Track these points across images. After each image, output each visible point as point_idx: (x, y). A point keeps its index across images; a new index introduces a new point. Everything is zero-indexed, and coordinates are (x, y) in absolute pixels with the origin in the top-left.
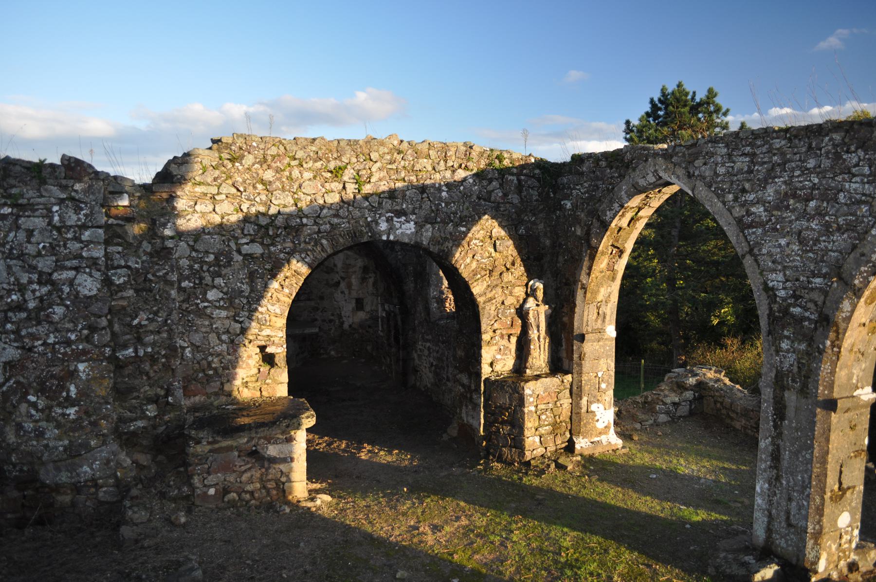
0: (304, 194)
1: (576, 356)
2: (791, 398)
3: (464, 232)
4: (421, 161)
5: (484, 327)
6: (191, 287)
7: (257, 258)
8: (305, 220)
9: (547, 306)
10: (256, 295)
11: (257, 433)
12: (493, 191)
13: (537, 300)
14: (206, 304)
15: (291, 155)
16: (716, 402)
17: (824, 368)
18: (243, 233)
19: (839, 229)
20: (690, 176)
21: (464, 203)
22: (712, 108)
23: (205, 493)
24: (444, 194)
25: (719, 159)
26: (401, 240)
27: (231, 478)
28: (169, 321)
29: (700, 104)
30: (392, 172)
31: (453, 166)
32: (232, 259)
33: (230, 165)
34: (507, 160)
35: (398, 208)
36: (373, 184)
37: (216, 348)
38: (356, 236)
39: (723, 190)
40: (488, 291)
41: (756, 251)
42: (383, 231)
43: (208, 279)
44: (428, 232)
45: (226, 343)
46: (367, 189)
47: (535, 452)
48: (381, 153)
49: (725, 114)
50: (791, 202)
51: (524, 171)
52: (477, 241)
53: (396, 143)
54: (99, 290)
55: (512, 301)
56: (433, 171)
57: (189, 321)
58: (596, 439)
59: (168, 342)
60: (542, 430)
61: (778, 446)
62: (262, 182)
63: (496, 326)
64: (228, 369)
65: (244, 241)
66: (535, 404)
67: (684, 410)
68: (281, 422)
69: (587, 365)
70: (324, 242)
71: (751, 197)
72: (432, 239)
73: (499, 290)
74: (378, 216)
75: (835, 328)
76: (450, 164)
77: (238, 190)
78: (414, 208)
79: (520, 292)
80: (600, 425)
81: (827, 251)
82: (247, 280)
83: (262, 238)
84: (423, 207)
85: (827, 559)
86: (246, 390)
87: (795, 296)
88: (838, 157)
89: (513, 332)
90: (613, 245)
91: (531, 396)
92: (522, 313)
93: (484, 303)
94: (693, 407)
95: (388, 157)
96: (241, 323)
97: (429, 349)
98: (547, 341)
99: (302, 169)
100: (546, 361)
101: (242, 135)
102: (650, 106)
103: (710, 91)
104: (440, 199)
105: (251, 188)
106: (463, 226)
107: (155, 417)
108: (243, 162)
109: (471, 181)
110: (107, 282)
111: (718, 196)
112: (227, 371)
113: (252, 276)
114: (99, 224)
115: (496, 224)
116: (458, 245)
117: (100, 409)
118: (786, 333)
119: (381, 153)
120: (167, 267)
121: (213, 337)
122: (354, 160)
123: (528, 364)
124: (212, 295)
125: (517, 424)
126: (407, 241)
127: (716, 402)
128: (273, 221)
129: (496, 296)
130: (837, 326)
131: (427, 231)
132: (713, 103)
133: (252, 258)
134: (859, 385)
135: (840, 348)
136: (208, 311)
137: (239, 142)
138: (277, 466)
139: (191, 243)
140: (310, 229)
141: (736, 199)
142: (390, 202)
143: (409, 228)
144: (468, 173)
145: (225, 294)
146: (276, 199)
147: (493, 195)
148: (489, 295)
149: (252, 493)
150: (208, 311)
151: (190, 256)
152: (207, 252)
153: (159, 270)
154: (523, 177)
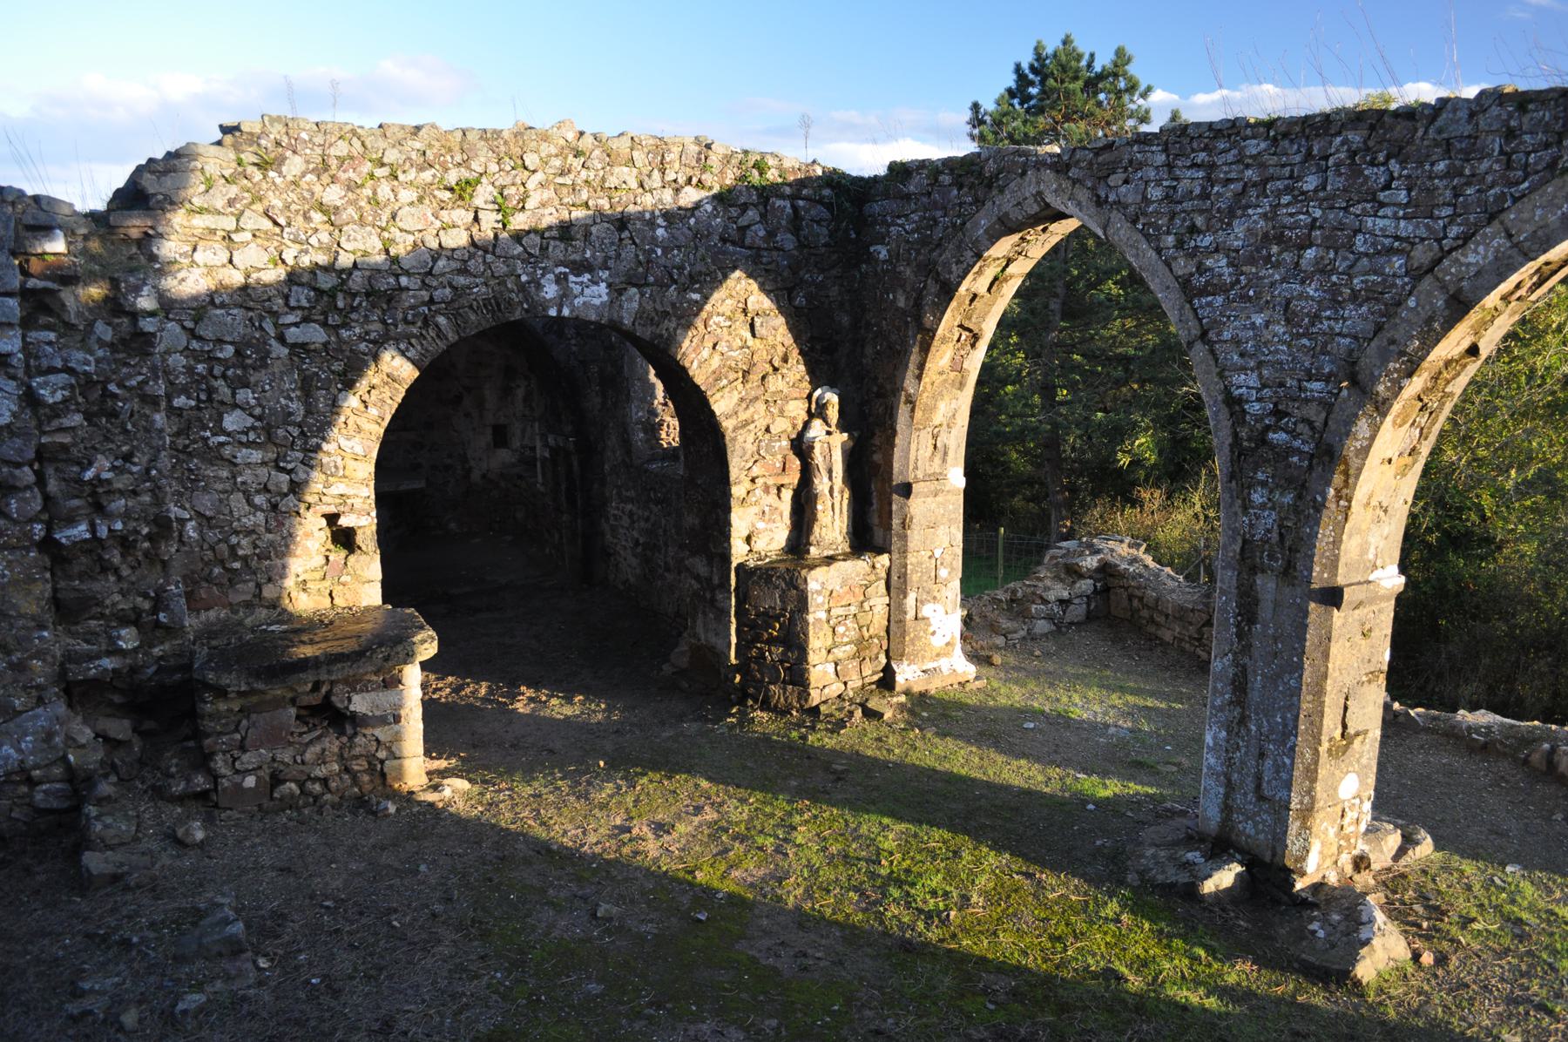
0: (401, 230)
1: (896, 522)
2: (1266, 585)
3: (697, 302)
4: (616, 170)
5: (734, 473)
6: (191, 408)
7: (315, 351)
8: (404, 281)
9: (845, 435)
10: (317, 421)
11: (329, 672)
12: (748, 226)
13: (828, 425)
14: (222, 439)
15: (374, 156)
16: (1131, 597)
17: (1324, 535)
18: (287, 304)
19: (1355, 296)
20: (1100, 202)
21: (696, 248)
22: (1122, 84)
23: (238, 787)
24: (660, 232)
25: (1152, 174)
26: (582, 315)
27: (286, 756)
28: (154, 472)
29: (1101, 77)
30: (565, 191)
31: (675, 181)
32: (269, 352)
33: (258, 176)
34: (773, 170)
35: (576, 257)
36: (528, 213)
37: (244, 520)
38: (500, 310)
39: (1157, 228)
41: (1212, 335)
42: (551, 300)
43: (224, 390)
44: (632, 301)
45: (263, 511)
46: (519, 222)
47: (826, 691)
48: (543, 155)
49: (1144, 95)
50: (1275, 249)
51: (805, 192)
52: (721, 319)
53: (571, 136)
54: (14, 415)
55: (784, 427)
56: (641, 190)
57: (190, 470)
58: (929, 665)
59: (154, 510)
60: (839, 653)
61: (1244, 667)
62: (321, 208)
63: (756, 471)
64: (269, 558)
65: (291, 319)
66: (826, 607)
67: (1077, 611)
68: (374, 651)
69: (915, 537)
70: (441, 320)
71: (1206, 241)
72: (640, 314)
73: (760, 406)
74: (539, 272)
75: (1342, 467)
76: (670, 176)
77: (276, 223)
78: (607, 258)
79: (798, 410)
80: (938, 642)
81: (1333, 335)
82: (298, 393)
83: (325, 313)
84: (623, 255)
85: (1321, 853)
86: (303, 596)
87: (1278, 413)
88: (1356, 172)
89: (786, 480)
90: (961, 326)
91: (819, 593)
92: (801, 447)
93: (735, 429)
94: (1092, 607)
95: (557, 163)
96: (289, 472)
97: (631, 514)
98: (846, 495)
99: (396, 183)
100: (845, 531)
101: (279, 117)
102: (1014, 77)
103: (1120, 53)
104: (654, 239)
105: (300, 219)
106: (695, 291)
107: (135, 650)
108: (284, 169)
109: (709, 208)
110: (30, 399)
111: (1147, 236)
112: (267, 562)
113: (307, 387)
114: (9, 288)
115: (754, 286)
116: (689, 326)
117: (30, 640)
118: (1260, 476)
119: (543, 155)
120: (145, 370)
121: (237, 502)
122: (493, 167)
123: (812, 538)
124: (232, 421)
125: (795, 643)
126: (593, 317)
127: (1131, 597)
128: (344, 282)
129: (756, 417)
130: (1347, 464)
131: (630, 299)
132: (1125, 74)
133: (308, 351)
134: (1379, 563)
135: (1350, 501)
136: (227, 451)
137: (274, 131)
138: (368, 731)
139: (189, 324)
140: (413, 297)
141: (1180, 244)
142: (562, 246)
143: (598, 294)
144: (704, 194)
145: (259, 418)
146: (348, 240)
147: (749, 234)
148: (743, 416)
149: (324, 781)
150: (227, 451)
151: (187, 348)
152: (220, 341)
153: (130, 377)
154: (801, 203)
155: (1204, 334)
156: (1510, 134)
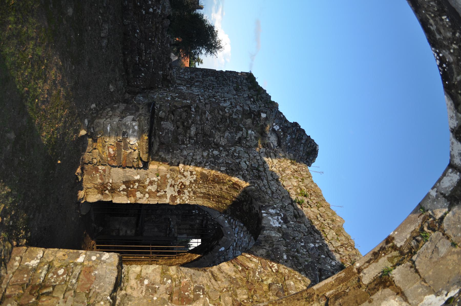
3: (282, 257)
24: (312, 245)
40: (224, 274)
52: (276, 267)
91: (99, 258)
93: (212, 272)
140: (260, 183)
148: (220, 276)
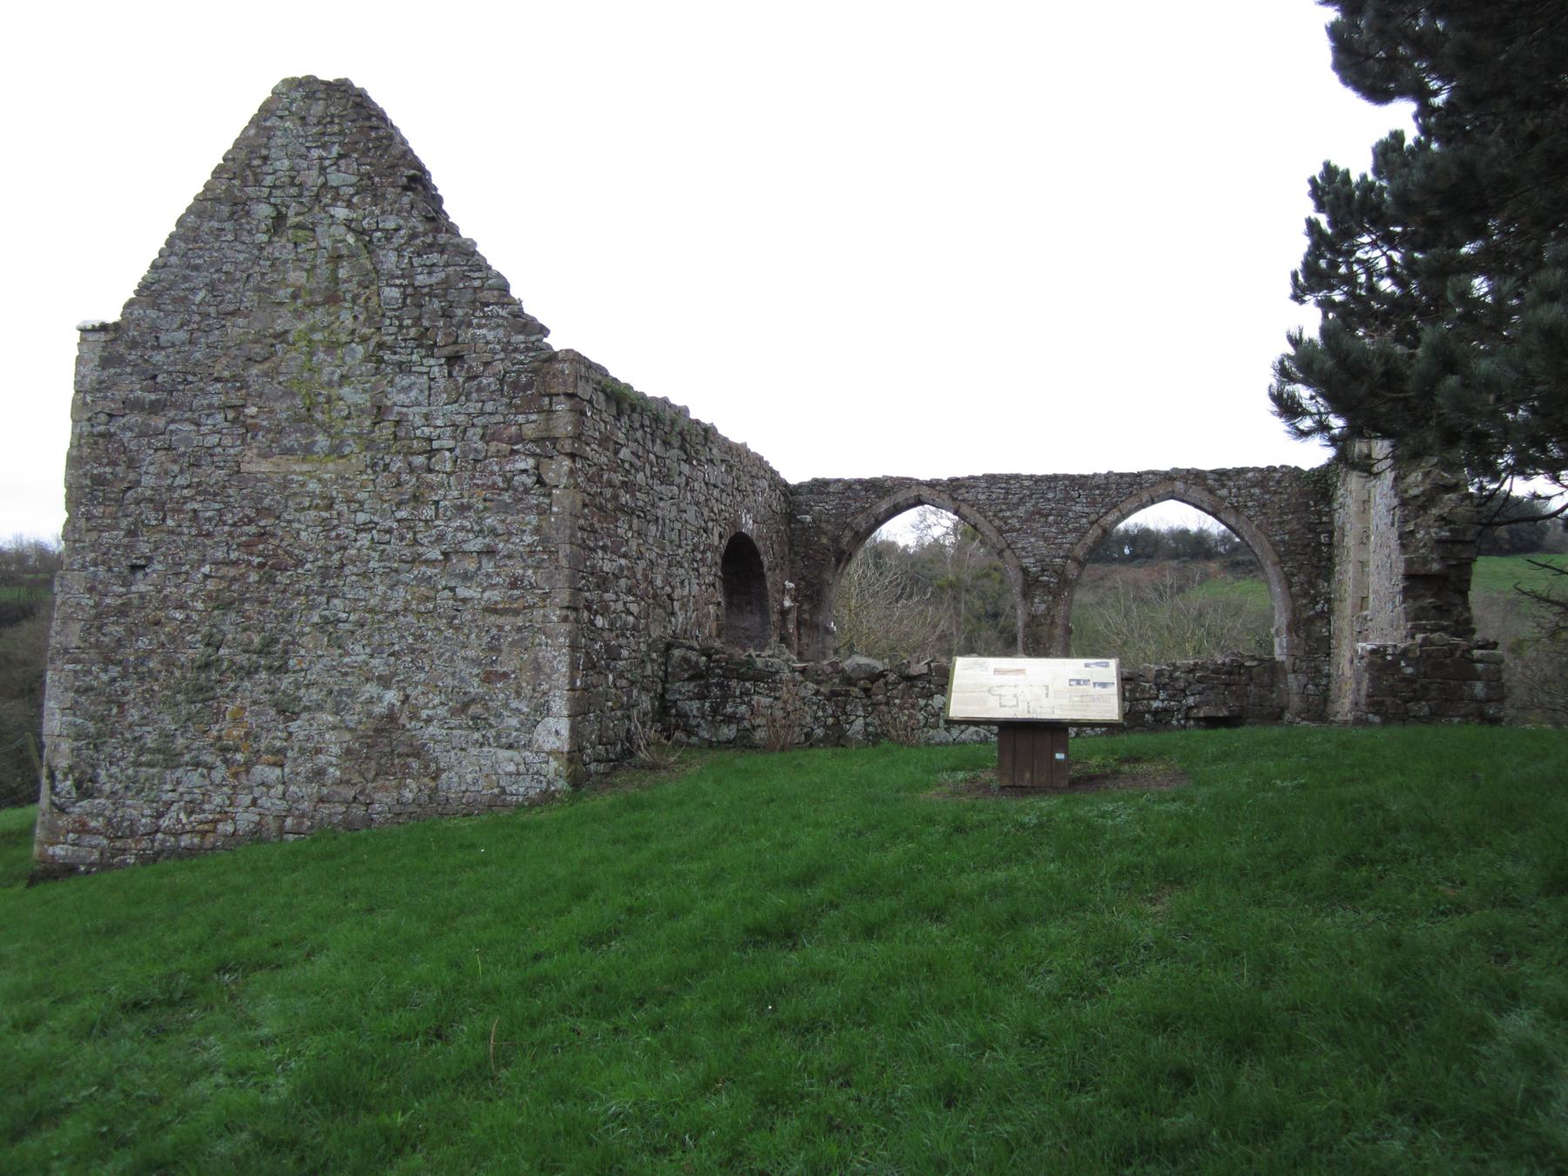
19: (1070, 531)
141: (995, 516)
155: (1009, 546)
156: (1118, 484)
